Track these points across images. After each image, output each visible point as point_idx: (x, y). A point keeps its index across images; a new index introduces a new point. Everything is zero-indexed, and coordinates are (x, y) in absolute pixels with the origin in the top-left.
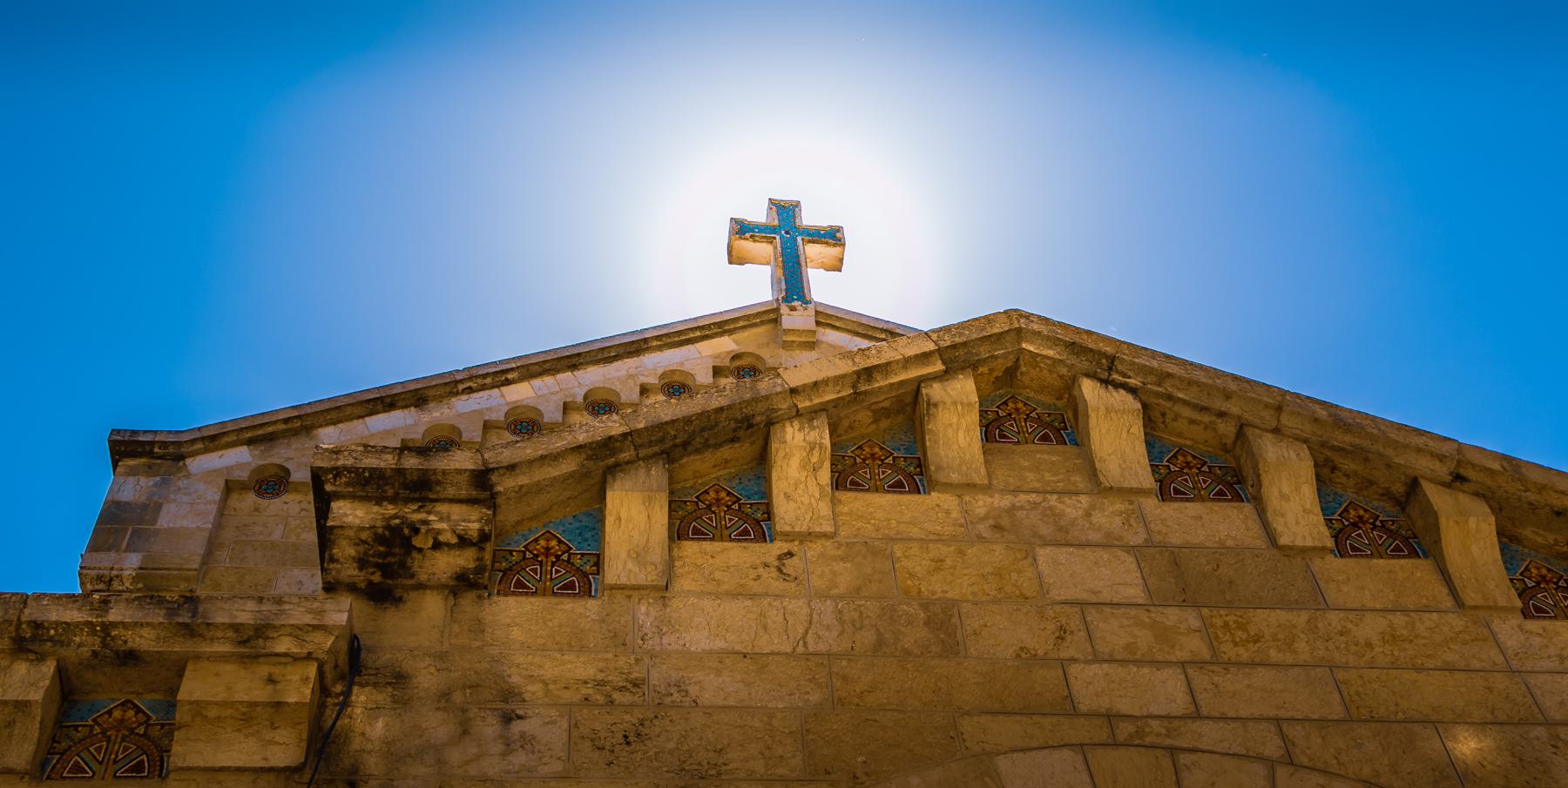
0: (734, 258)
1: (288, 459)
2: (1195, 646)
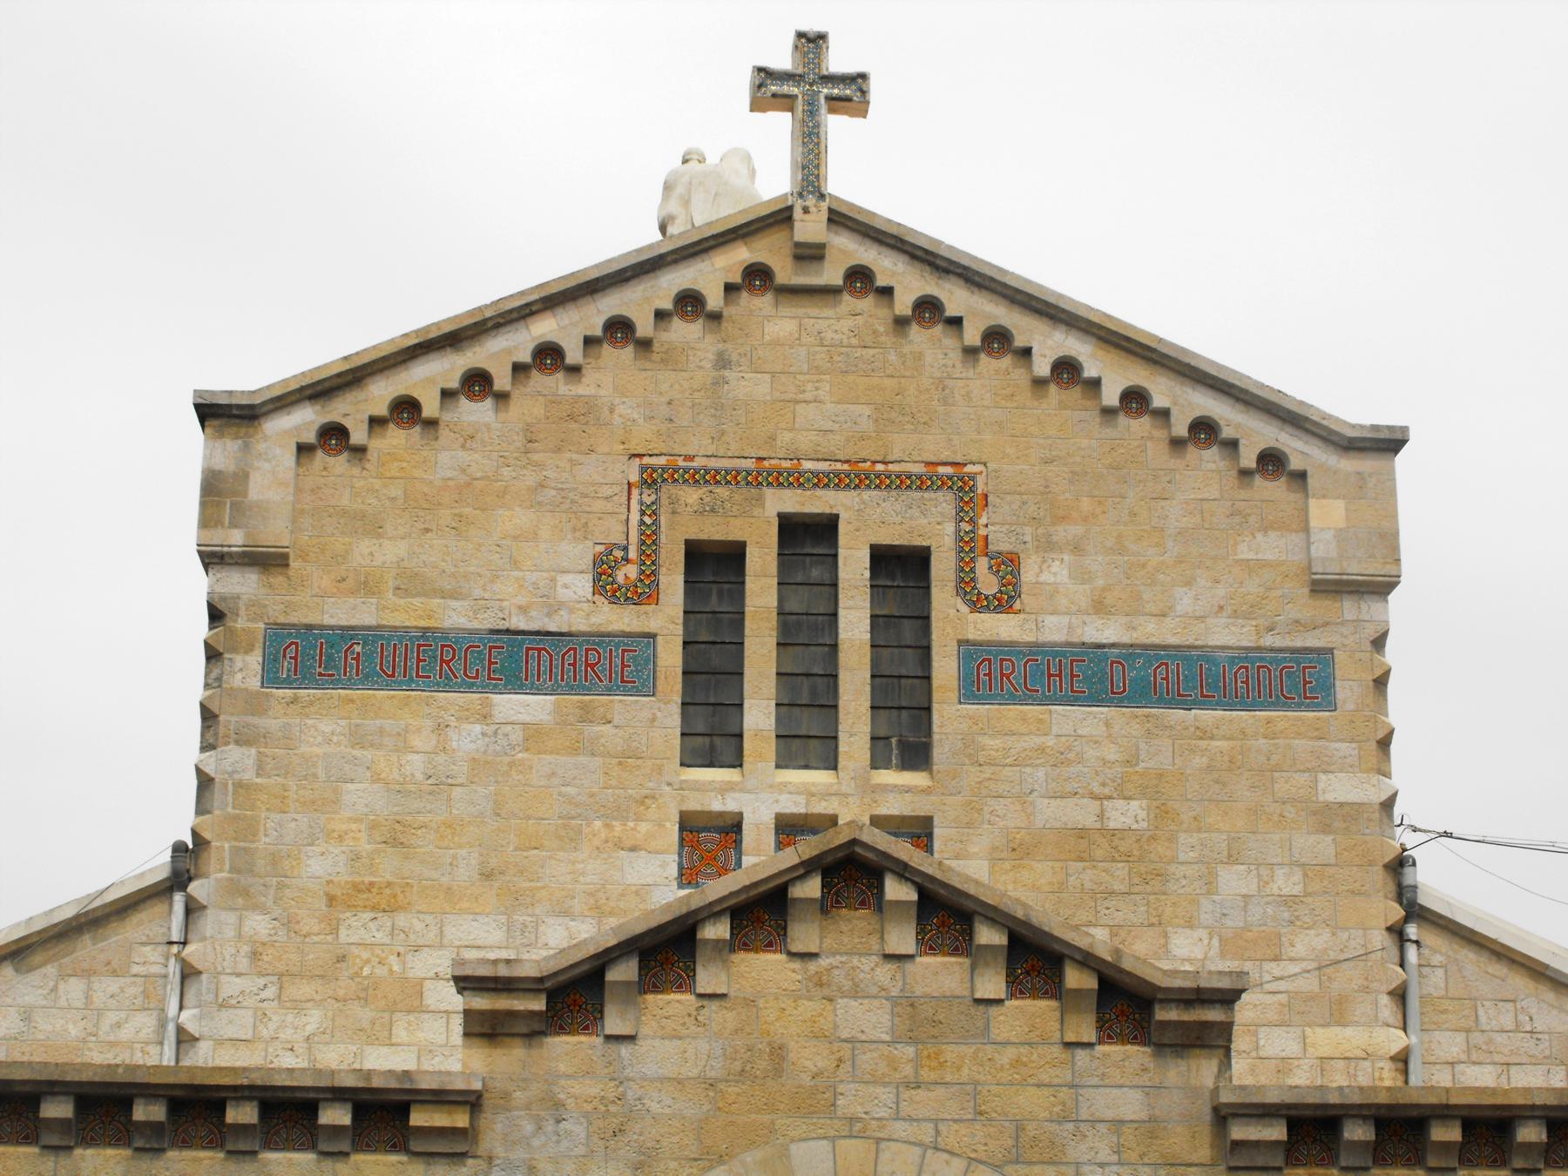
0: (757, 105)
1: (346, 415)
2: (908, 1070)
